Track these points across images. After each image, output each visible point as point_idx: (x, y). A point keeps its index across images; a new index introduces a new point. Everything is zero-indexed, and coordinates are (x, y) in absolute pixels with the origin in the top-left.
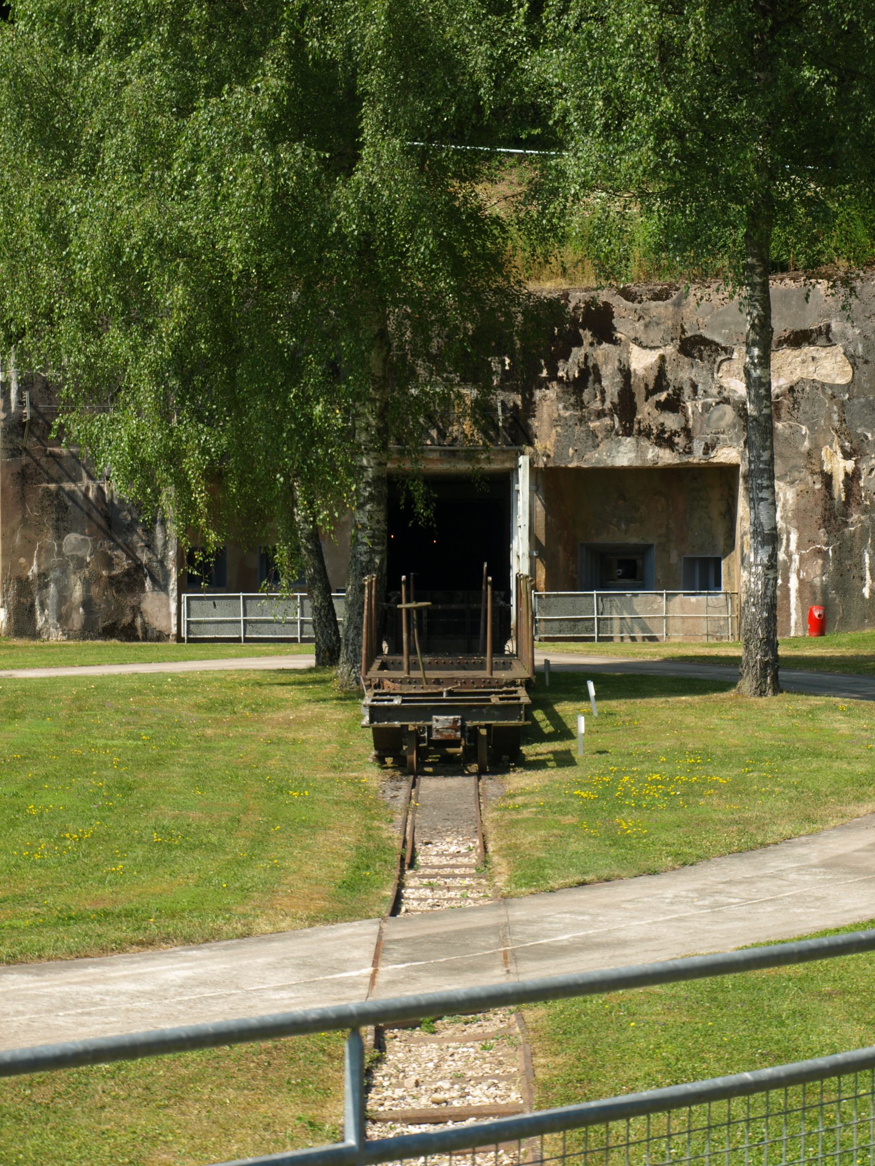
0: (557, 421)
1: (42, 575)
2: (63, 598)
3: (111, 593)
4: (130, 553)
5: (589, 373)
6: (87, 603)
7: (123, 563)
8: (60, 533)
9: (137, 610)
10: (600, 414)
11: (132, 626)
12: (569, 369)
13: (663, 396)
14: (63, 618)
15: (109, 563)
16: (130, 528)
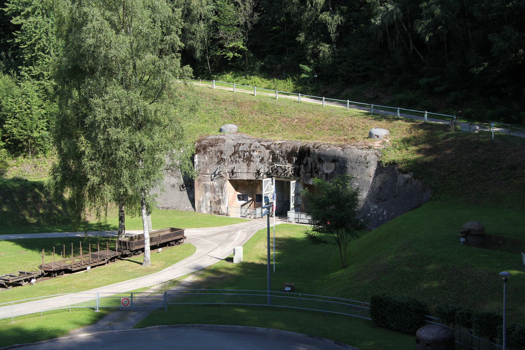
0: (303, 173)
1: (203, 200)
2: (206, 205)
3: (215, 205)
4: (218, 196)
5: (307, 163)
6: (211, 206)
7: (217, 199)
8: (206, 192)
9: (220, 208)
10: (308, 173)
11: (219, 211)
12: (305, 162)
13: (316, 170)
14: (206, 209)
15: (214, 198)
16: (218, 192)
